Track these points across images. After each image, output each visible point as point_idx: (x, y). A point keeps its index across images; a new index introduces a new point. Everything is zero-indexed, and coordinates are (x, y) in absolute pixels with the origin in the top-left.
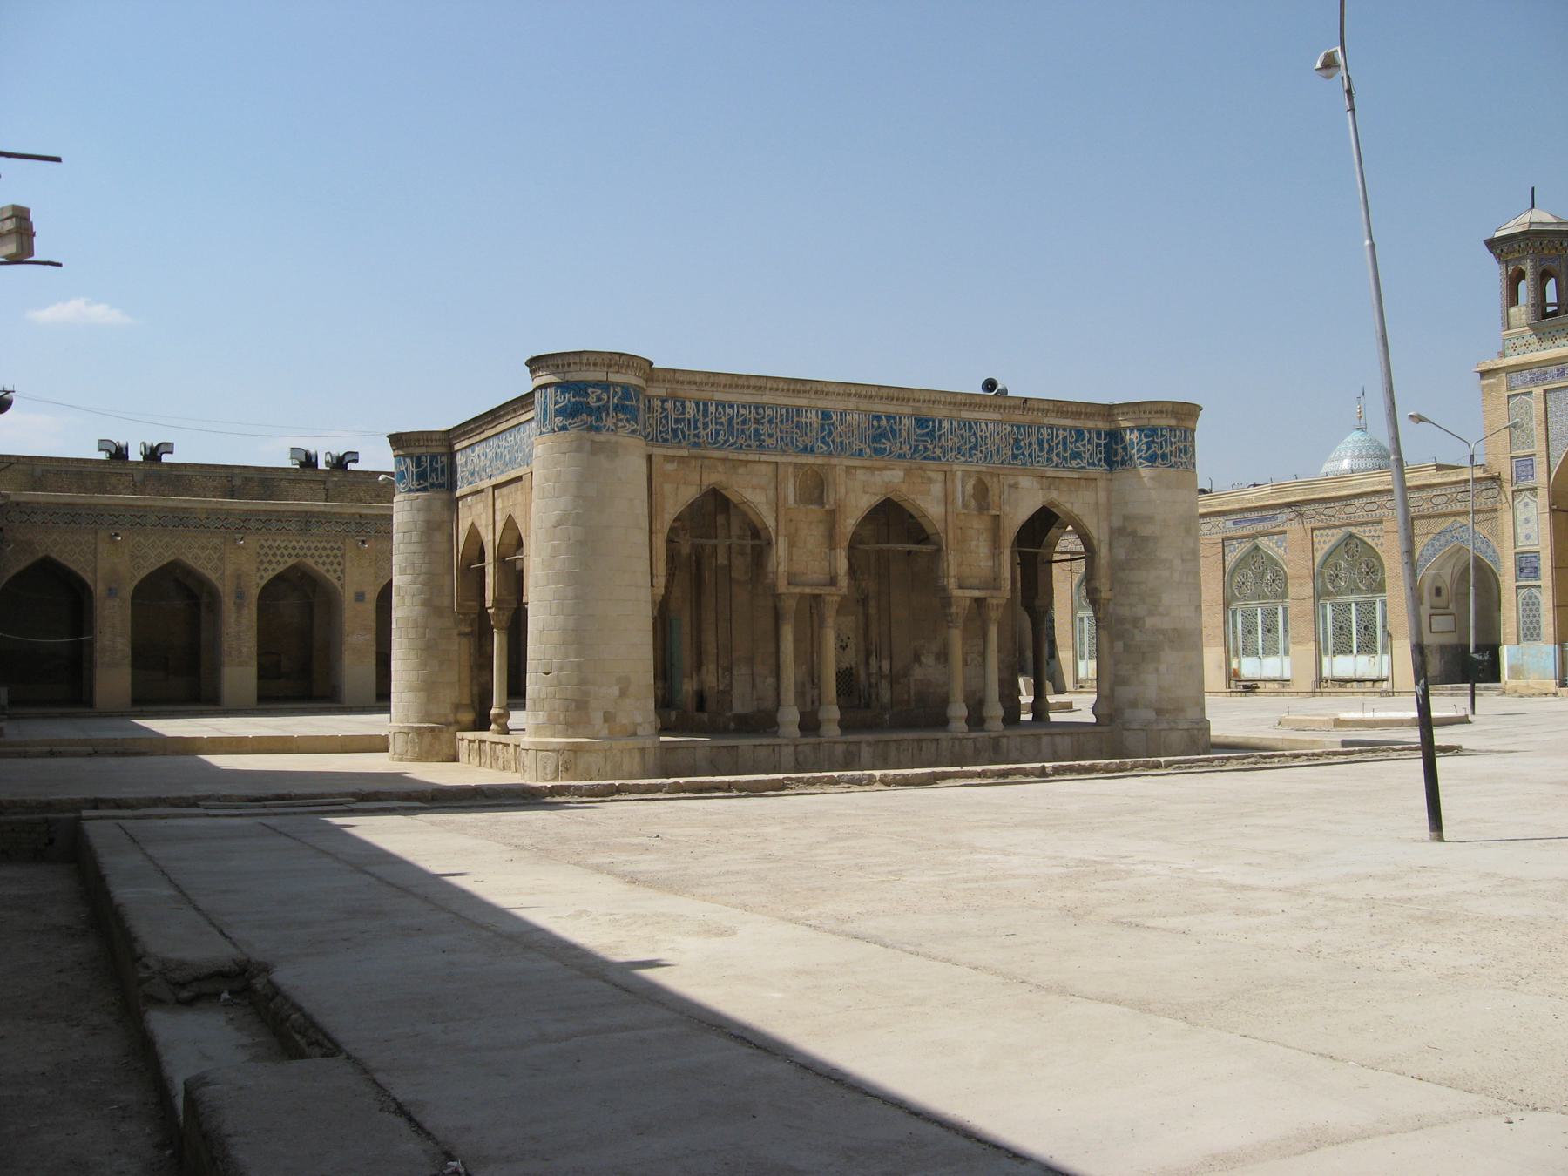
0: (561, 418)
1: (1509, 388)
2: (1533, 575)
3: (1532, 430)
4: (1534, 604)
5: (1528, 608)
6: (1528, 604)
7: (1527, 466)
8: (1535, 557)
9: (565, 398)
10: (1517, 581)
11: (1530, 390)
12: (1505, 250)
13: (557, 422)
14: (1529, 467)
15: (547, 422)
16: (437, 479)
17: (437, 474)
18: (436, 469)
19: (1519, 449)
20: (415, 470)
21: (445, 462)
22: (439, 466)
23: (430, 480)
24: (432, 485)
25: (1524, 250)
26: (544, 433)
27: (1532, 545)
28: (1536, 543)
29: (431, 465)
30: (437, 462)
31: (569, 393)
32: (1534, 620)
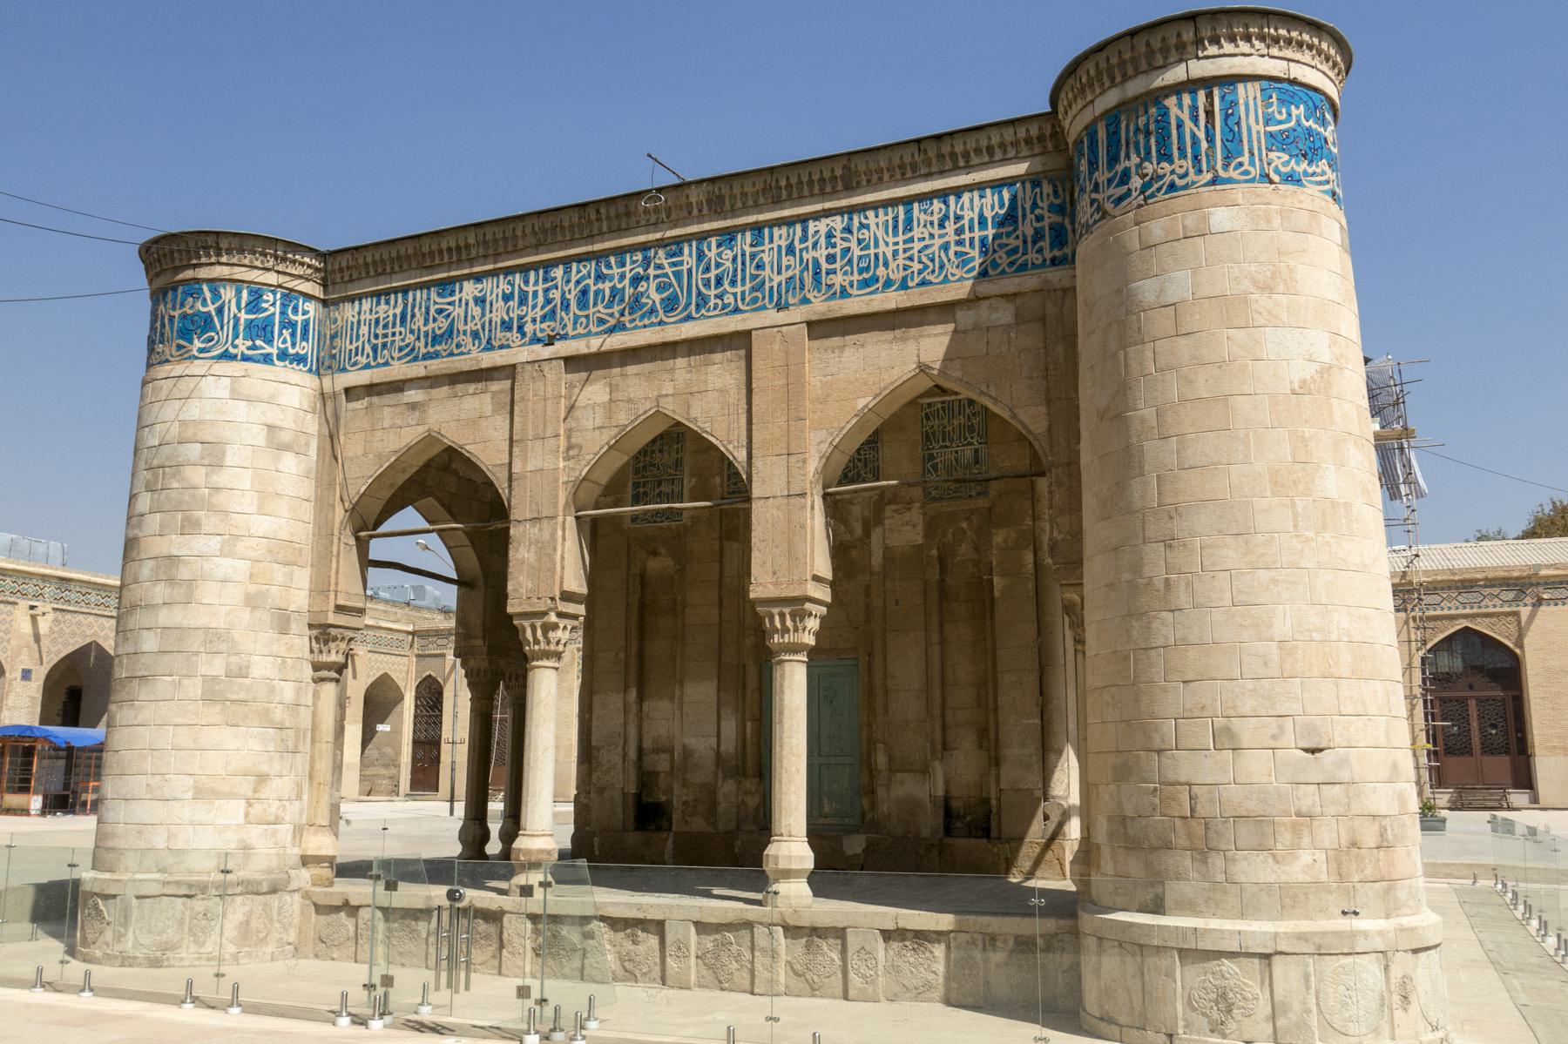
0: (1286, 157)
9: (1290, 115)
13: (1277, 162)
15: (1245, 159)
16: (294, 345)
17: (293, 335)
18: (293, 325)
20: (243, 316)
21: (312, 314)
22: (300, 318)
23: (278, 343)
24: (283, 355)
26: (1230, 181)
29: (282, 313)
30: (295, 310)
31: (1298, 108)
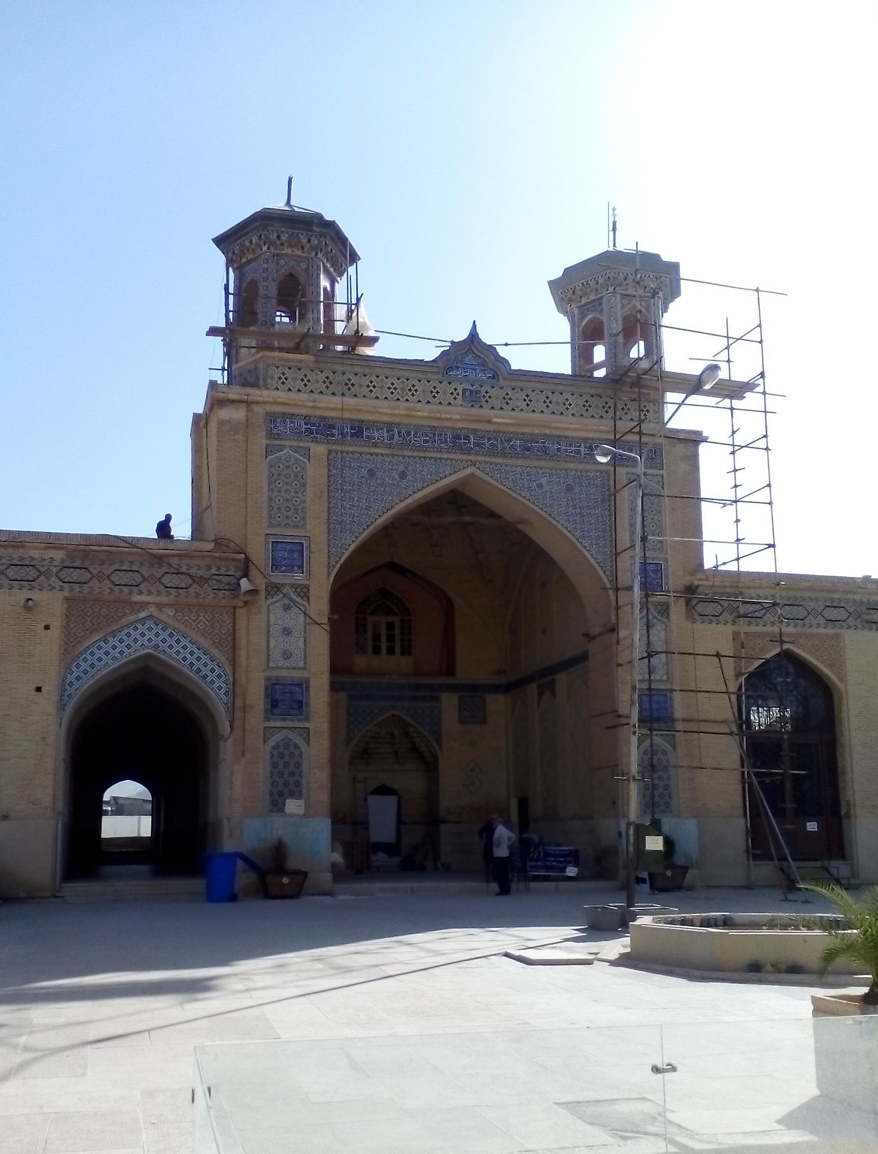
1: (270, 435)
2: (295, 712)
3: (304, 502)
4: (292, 755)
5: (281, 762)
6: (281, 756)
7: (291, 551)
8: (300, 685)
10: (267, 719)
11: (306, 445)
12: (284, 238)
14: (296, 555)
19: (279, 525)
25: (312, 248)
27: (294, 668)
28: (301, 664)
32: (292, 781)
